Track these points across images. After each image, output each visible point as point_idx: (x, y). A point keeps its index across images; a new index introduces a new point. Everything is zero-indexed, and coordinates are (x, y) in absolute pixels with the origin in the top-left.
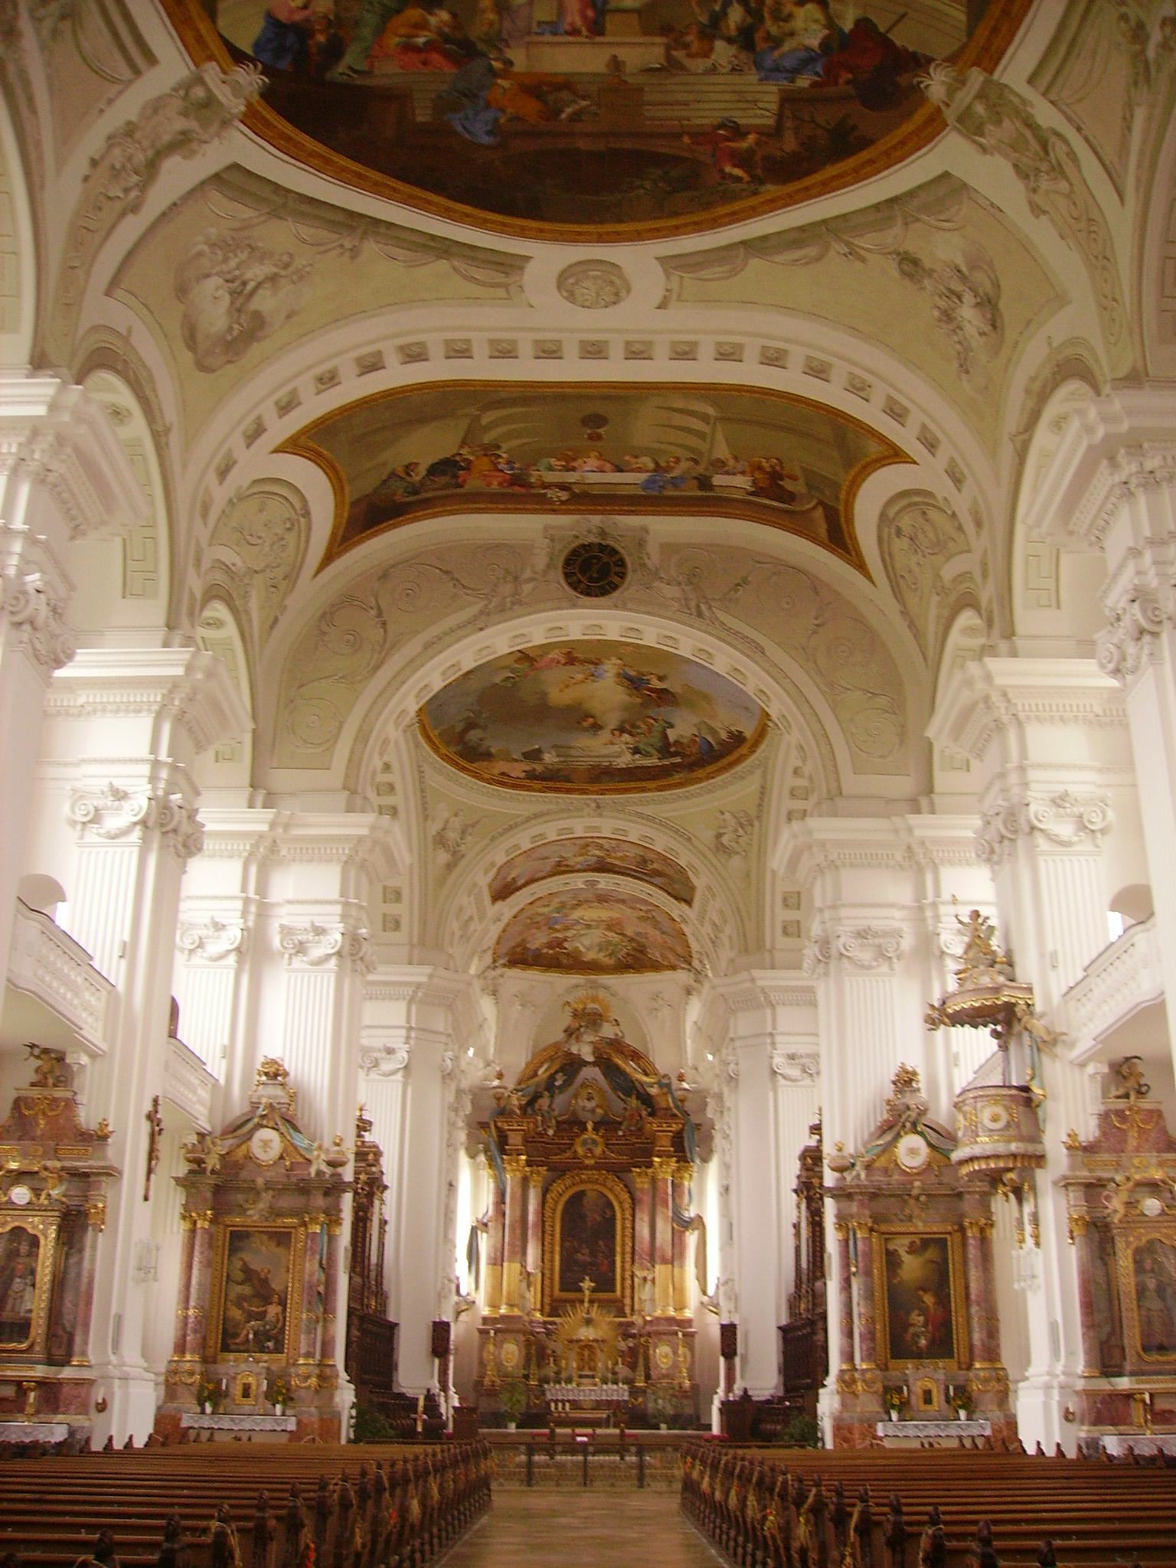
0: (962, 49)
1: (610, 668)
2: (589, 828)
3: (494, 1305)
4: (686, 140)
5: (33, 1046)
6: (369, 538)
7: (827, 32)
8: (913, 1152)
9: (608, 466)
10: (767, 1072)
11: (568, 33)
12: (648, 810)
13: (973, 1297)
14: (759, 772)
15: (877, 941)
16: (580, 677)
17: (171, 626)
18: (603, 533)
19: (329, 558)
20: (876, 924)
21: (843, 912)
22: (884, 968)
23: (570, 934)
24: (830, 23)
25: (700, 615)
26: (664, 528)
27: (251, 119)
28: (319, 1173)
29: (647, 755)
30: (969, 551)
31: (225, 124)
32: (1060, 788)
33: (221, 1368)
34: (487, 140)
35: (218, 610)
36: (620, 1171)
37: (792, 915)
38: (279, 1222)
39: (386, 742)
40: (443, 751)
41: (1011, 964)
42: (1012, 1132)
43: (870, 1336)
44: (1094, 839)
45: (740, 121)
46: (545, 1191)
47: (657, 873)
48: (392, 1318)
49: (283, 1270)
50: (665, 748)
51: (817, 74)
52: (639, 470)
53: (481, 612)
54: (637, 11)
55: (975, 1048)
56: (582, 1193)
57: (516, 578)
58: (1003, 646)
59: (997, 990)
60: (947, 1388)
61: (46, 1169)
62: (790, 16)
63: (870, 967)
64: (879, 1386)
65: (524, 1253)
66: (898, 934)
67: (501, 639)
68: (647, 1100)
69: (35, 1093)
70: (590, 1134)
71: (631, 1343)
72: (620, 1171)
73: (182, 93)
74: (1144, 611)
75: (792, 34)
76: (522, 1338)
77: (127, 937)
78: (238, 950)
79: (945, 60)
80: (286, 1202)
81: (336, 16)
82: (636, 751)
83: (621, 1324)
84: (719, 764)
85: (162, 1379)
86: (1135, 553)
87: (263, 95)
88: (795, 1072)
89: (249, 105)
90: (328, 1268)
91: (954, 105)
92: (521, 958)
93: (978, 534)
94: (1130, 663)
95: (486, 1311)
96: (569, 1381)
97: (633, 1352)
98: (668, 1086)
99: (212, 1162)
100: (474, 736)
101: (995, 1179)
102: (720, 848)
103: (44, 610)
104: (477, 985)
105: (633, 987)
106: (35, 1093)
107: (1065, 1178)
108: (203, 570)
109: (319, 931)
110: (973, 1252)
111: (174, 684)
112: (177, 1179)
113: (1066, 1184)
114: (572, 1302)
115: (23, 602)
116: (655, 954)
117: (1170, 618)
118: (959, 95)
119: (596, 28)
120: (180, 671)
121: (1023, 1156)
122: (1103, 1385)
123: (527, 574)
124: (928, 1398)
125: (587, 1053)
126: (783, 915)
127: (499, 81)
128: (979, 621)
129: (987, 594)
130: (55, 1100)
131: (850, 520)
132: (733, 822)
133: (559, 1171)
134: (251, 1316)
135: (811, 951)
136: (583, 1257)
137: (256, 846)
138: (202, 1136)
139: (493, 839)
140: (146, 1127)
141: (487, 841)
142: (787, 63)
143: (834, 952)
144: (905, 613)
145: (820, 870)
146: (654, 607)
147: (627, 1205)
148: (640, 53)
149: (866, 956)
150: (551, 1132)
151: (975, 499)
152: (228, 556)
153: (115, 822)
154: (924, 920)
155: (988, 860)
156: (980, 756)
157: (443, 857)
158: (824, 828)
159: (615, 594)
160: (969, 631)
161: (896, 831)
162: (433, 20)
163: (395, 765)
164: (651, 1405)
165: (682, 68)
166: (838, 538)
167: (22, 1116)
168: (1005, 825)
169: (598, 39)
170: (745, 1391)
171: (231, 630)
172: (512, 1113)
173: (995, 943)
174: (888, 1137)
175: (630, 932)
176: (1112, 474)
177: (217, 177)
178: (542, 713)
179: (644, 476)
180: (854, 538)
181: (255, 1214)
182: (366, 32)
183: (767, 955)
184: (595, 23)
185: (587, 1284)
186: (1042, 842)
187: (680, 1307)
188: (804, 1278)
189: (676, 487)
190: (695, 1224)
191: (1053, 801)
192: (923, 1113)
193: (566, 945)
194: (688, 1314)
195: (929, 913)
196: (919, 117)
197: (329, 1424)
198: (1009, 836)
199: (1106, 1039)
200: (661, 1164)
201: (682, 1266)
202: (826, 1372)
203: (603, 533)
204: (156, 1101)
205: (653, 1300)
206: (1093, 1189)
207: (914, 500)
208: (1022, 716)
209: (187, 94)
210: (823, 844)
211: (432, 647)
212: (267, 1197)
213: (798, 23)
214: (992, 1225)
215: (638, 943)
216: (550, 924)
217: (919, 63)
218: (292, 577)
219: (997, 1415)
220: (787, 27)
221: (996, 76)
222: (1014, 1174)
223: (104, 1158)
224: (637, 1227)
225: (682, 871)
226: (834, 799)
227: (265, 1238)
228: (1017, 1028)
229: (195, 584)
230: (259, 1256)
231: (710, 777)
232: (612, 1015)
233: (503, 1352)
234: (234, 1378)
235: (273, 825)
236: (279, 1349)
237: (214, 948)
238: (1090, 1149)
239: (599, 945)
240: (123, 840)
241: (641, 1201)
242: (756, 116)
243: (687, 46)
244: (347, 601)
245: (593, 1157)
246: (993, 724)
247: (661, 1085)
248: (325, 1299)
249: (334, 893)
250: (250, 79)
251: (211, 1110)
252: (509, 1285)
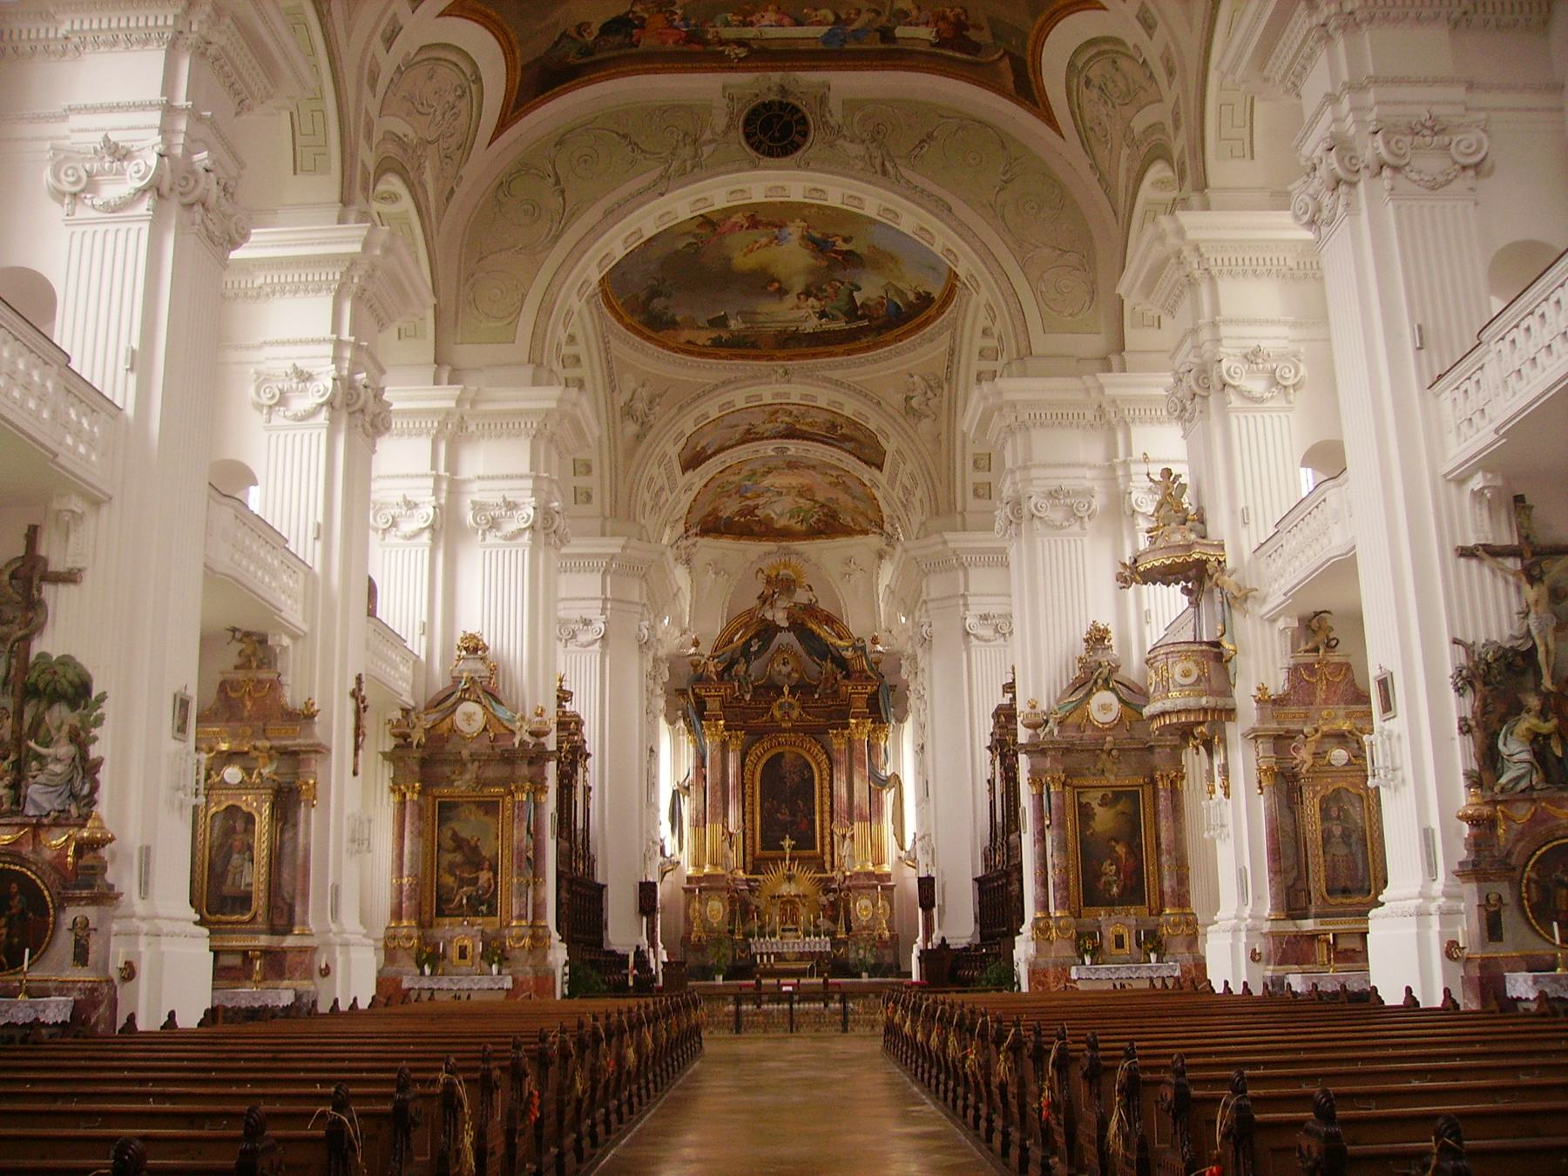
1: (794, 231)
2: (776, 395)
3: (698, 865)
5: (234, 630)
6: (543, 103)
8: (1105, 708)
9: (786, 20)
10: (960, 632)
12: (837, 374)
13: (1163, 847)
14: (947, 334)
15: (1068, 501)
16: (764, 240)
17: (345, 201)
18: (783, 90)
19: (502, 125)
20: (1067, 485)
21: (1034, 473)
22: (1076, 528)
23: (761, 501)
25: (885, 173)
26: (847, 84)
28: (522, 743)
29: (834, 318)
30: (1161, 101)
32: (1253, 344)
33: (437, 933)
35: (393, 183)
36: (817, 733)
37: (982, 477)
38: (486, 791)
39: (570, 313)
40: (627, 320)
41: (1202, 522)
42: (1203, 686)
43: (1063, 885)
44: (1286, 395)
46: (744, 755)
47: (845, 438)
48: (599, 880)
49: (492, 837)
50: (852, 312)
52: (819, 23)
53: (662, 177)
55: (1169, 601)
56: (780, 756)
57: (695, 141)
58: (1195, 198)
59: (1188, 547)
60: (1138, 933)
61: (255, 748)
63: (1061, 527)
64: (1072, 932)
65: (726, 815)
66: (1090, 493)
67: (680, 205)
68: (841, 663)
69: (240, 675)
70: (786, 698)
71: (831, 897)
72: (817, 733)
74: (1341, 160)
76: (725, 895)
77: (320, 519)
78: (432, 527)
80: (490, 772)
82: (822, 315)
83: (821, 879)
84: (908, 326)
85: (381, 944)
86: (1333, 99)
88: (987, 632)
90: (536, 834)
92: (713, 526)
93: (1170, 84)
94: (1325, 214)
95: (690, 871)
96: (773, 934)
97: (834, 905)
98: (863, 649)
99: (418, 736)
100: (658, 304)
101: (1185, 733)
102: (909, 411)
103: (215, 191)
104: (670, 554)
105: (825, 554)
106: (240, 675)
107: (1254, 730)
108: (375, 140)
109: (512, 506)
110: (1163, 804)
111: (353, 262)
112: (384, 754)
113: (1255, 736)
114: (774, 860)
115: (192, 183)
116: (846, 519)
117: (1367, 167)
120: (357, 248)
121: (1214, 710)
122: (1289, 927)
123: (707, 135)
124: (1119, 942)
125: (781, 619)
126: (974, 477)
128: (1169, 173)
129: (1178, 145)
130: (259, 682)
131: (1038, 72)
132: (923, 385)
133: (756, 735)
134: (463, 882)
135: (1002, 513)
136: (784, 816)
137: (443, 424)
138: (406, 712)
139: (681, 408)
140: (350, 705)
141: (675, 410)
143: (1025, 511)
144: (1094, 167)
145: (1011, 431)
146: (842, 167)
147: (824, 766)
149: (1058, 516)
150: (748, 697)
151: (1167, 47)
152: (400, 127)
153: (301, 404)
154: (1115, 479)
155: (1180, 418)
156: (1172, 313)
157: (632, 428)
158: (1015, 388)
159: (799, 154)
160: (1161, 184)
161: (1087, 390)
163: (580, 336)
164: (852, 955)
166: (1027, 91)
167: (227, 698)
168: (1197, 380)
170: (943, 939)
171: (406, 203)
172: (709, 679)
173: (1187, 500)
174: (1080, 694)
175: (820, 497)
176: (1309, 16)
178: (728, 279)
179: (825, 29)
180: (1042, 90)
181: (462, 785)
183: (959, 518)
185: (787, 843)
186: (1235, 400)
187: (879, 861)
188: (999, 832)
189: (857, 40)
191: (1246, 356)
192: (1114, 670)
194: (887, 868)
195: (1120, 473)
197: (544, 981)
198: (1200, 393)
199: (1294, 595)
201: (879, 823)
202: (1022, 921)
203: (783, 90)
204: (359, 679)
205: (852, 856)
206: (1281, 741)
207: (1104, 48)
208: (1214, 271)
210: (1013, 405)
211: (613, 214)
212: (473, 768)
214: (1183, 778)
215: (830, 509)
216: (741, 492)
218: (466, 147)
219: (1187, 958)
222: (1204, 728)
223: (312, 735)
225: (871, 436)
226: (1024, 358)
227: (473, 807)
228: (1208, 584)
229: (367, 157)
230: (468, 825)
231: (899, 339)
232: (805, 582)
234: (451, 941)
235: (459, 402)
236: (492, 911)
237: (408, 527)
238: (1279, 701)
239: (791, 511)
240: (311, 421)
241: (839, 763)
244: (524, 168)
245: (790, 719)
246: (1185, 279)
247: (855, 649)
248: (535, 863)
249: (525, 468)
251: (413, 687)
252: (712, 844)
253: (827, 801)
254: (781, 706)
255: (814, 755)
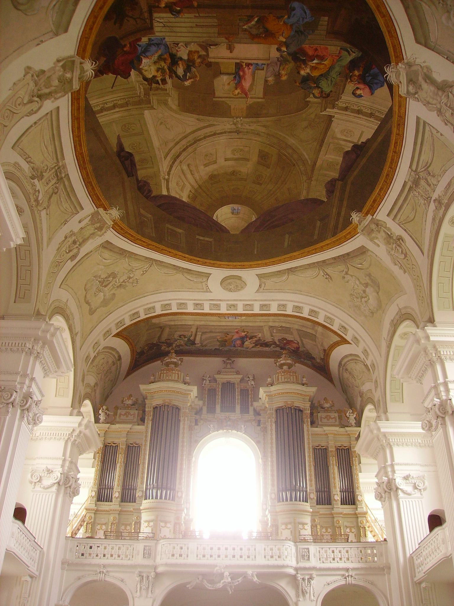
0: (86, 91)
4: (195, 4)
7: (141, 67)
11: (252, 65)
24: (140, 71)
27: (400, 58)
31: (409, 65)
34: (296, 4)
45: (170, 15)
51: (140, 46)
54: (221, 73)
62: (158, 71)
73: (416, 96)
75: (155, 63)
79: (90, 81)
81: (347, 79)
87: (390, 63)
89: (397, 64)
91: (78, 66)
118: (79, 72)
119: (239, 66)
127: (284, 40)
142: (153, 48)
148: (219, 53)
162: (308, 70)
165: (200, 46)
169: (238, 61)
177: (426, 45)
182: (337, 69)
184: (239, 69)
196: (89, 48)
209: (416, 93)
213: (153, 68)
217: (99, 72)
220: (158, 66)
221: (70, 94)
242: (163, 18)
243: (200, 57)
250: (391, 73)
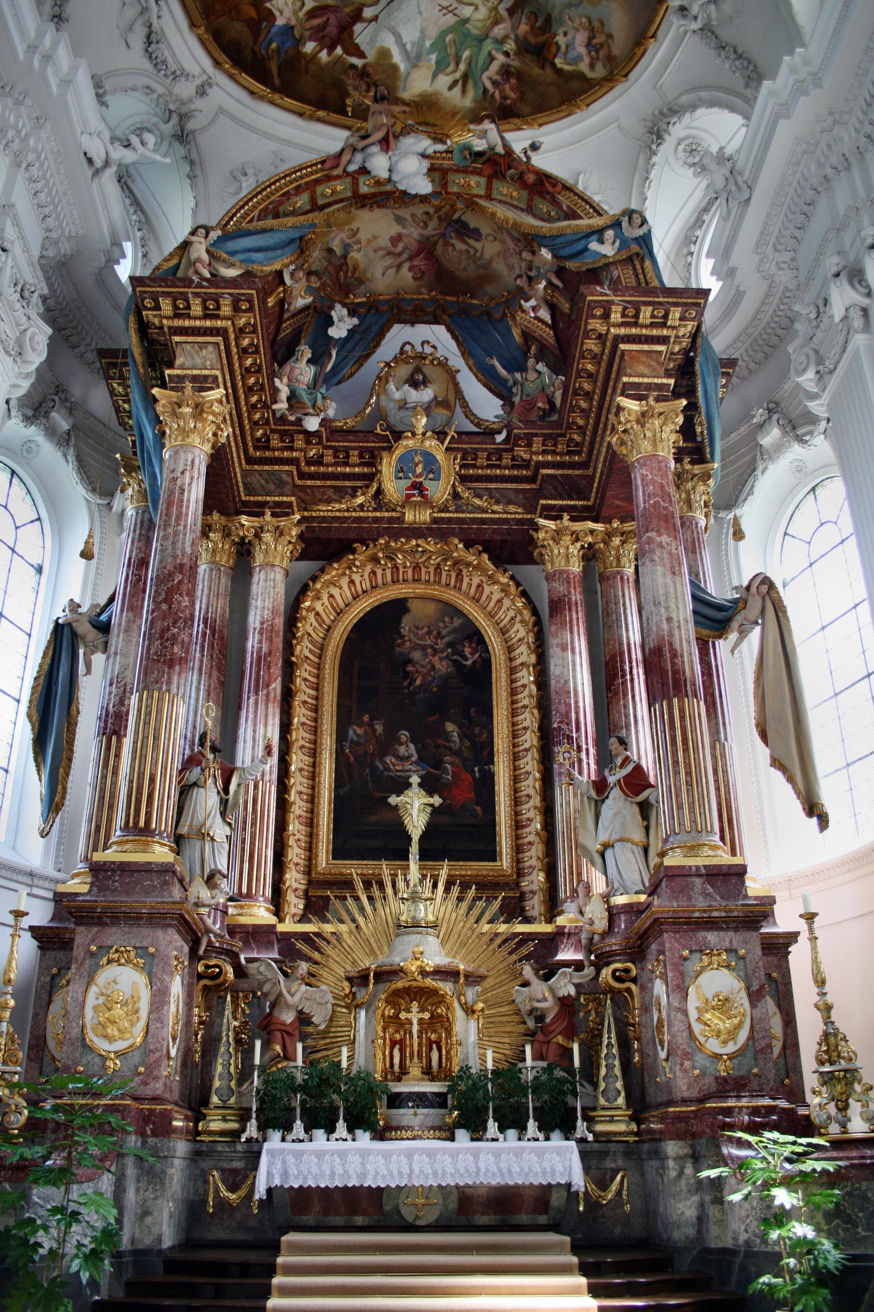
147: (520, 632)
190: (755, 604)
193: (362, 34)
200: (643, 418)
224: (554, 668)
233: (92, 1000)
239: (439, 44)
253: (529, 719)
254: (401, 471)
255: (492, 603)
